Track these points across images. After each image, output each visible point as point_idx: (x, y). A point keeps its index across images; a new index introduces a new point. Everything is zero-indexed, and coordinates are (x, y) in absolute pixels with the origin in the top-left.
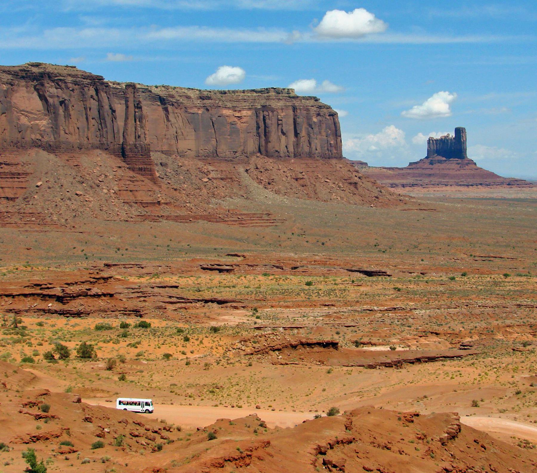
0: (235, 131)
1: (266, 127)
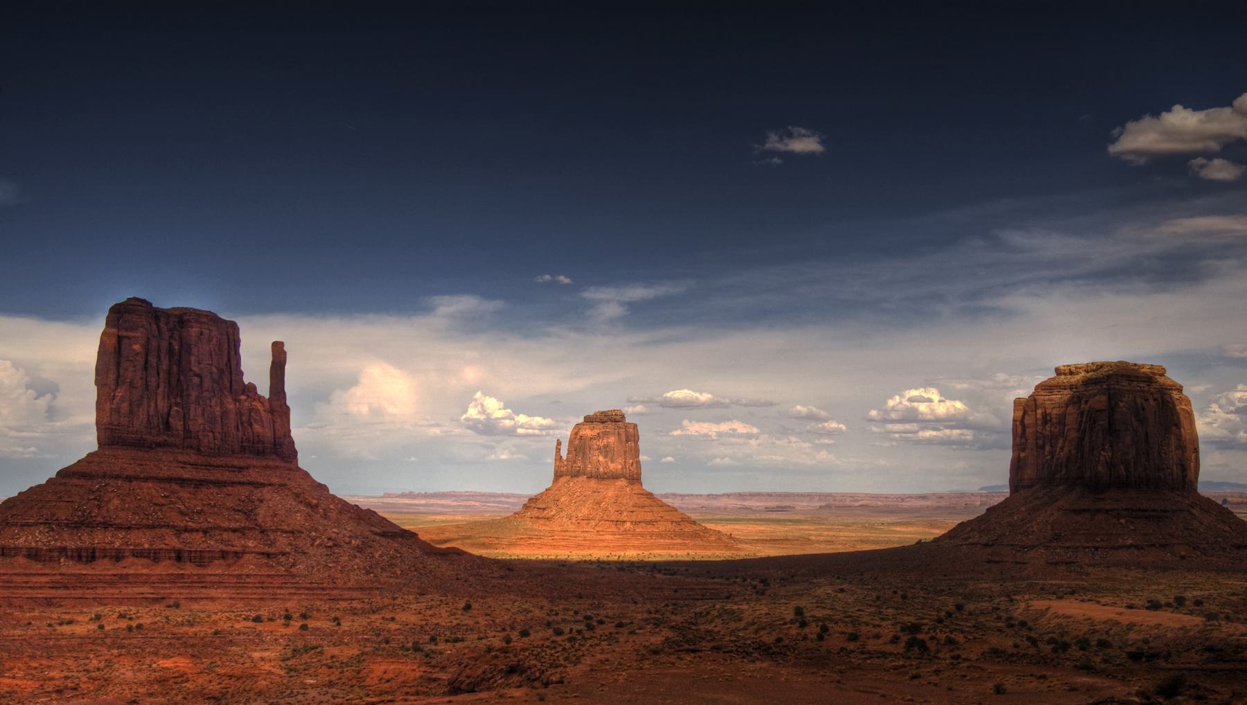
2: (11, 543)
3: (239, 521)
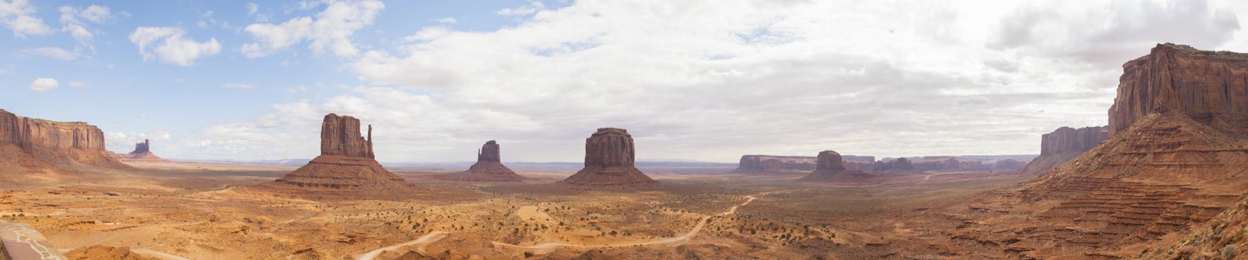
2: (294, 181)
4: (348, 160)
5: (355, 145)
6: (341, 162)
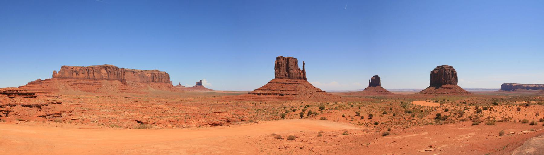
0: (147, 77)
1: (153, 77)
3: (293, 89)
4: (290, 81)
5: (294, 73)
6: (286, 82)
